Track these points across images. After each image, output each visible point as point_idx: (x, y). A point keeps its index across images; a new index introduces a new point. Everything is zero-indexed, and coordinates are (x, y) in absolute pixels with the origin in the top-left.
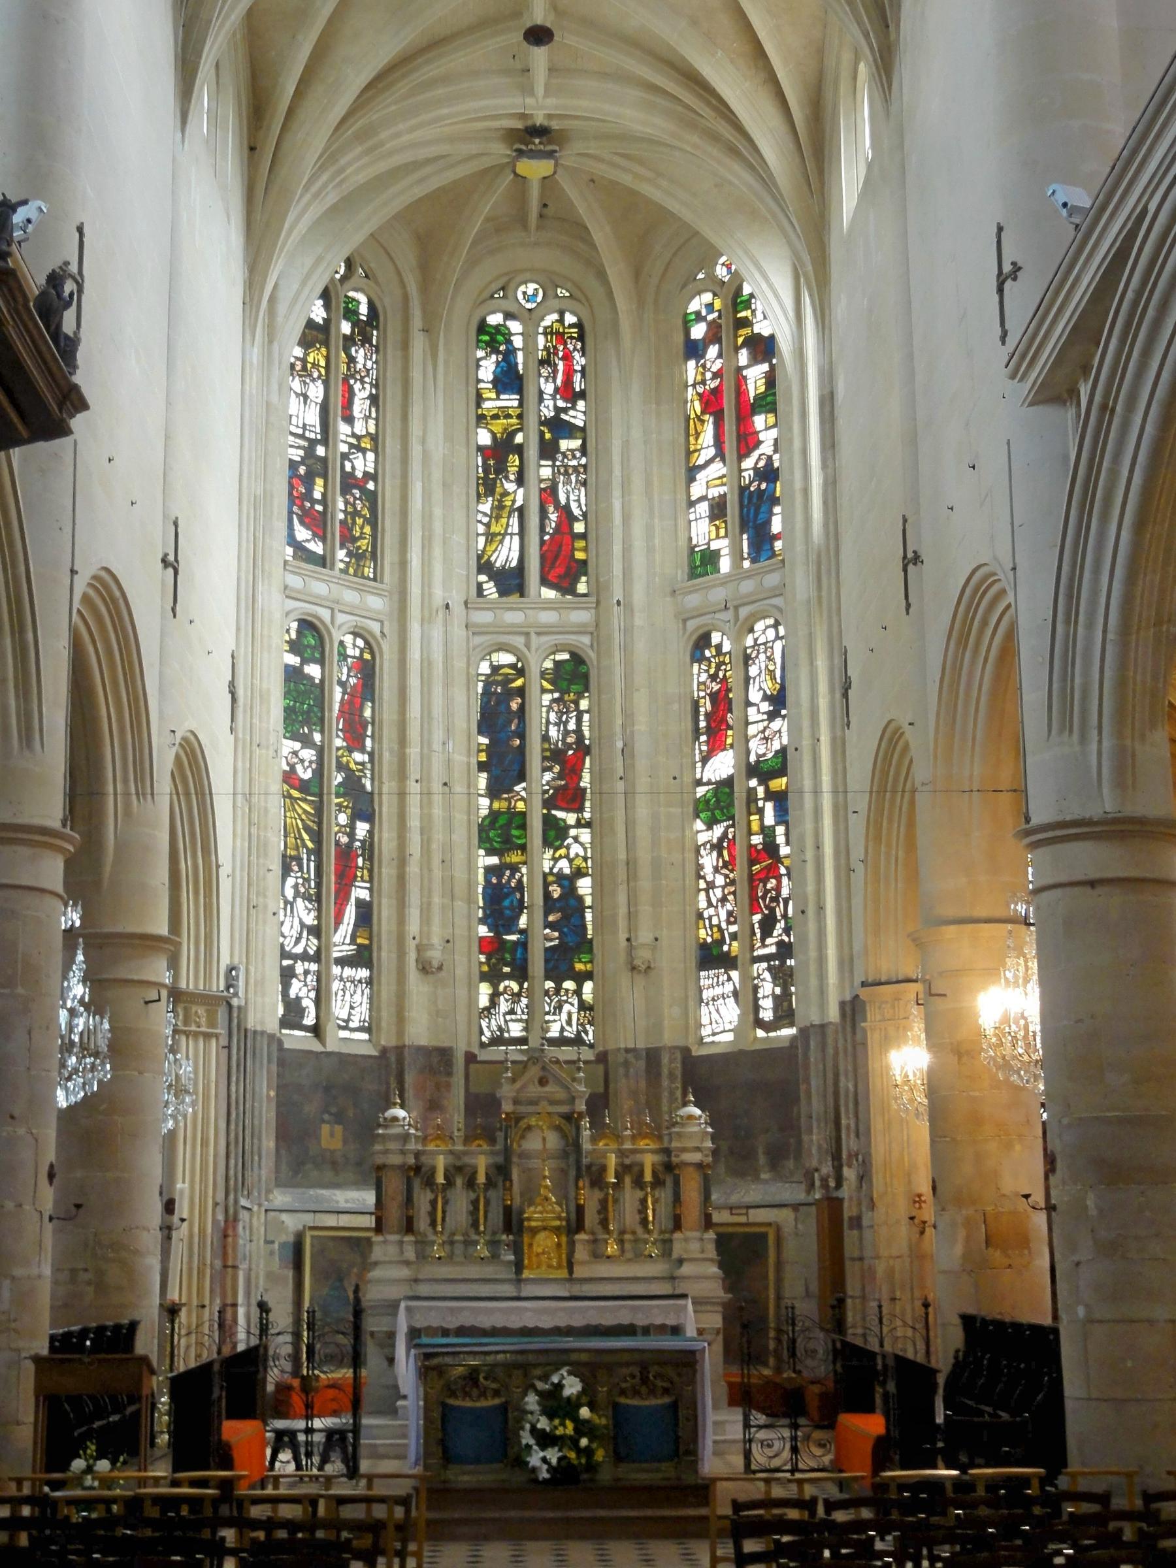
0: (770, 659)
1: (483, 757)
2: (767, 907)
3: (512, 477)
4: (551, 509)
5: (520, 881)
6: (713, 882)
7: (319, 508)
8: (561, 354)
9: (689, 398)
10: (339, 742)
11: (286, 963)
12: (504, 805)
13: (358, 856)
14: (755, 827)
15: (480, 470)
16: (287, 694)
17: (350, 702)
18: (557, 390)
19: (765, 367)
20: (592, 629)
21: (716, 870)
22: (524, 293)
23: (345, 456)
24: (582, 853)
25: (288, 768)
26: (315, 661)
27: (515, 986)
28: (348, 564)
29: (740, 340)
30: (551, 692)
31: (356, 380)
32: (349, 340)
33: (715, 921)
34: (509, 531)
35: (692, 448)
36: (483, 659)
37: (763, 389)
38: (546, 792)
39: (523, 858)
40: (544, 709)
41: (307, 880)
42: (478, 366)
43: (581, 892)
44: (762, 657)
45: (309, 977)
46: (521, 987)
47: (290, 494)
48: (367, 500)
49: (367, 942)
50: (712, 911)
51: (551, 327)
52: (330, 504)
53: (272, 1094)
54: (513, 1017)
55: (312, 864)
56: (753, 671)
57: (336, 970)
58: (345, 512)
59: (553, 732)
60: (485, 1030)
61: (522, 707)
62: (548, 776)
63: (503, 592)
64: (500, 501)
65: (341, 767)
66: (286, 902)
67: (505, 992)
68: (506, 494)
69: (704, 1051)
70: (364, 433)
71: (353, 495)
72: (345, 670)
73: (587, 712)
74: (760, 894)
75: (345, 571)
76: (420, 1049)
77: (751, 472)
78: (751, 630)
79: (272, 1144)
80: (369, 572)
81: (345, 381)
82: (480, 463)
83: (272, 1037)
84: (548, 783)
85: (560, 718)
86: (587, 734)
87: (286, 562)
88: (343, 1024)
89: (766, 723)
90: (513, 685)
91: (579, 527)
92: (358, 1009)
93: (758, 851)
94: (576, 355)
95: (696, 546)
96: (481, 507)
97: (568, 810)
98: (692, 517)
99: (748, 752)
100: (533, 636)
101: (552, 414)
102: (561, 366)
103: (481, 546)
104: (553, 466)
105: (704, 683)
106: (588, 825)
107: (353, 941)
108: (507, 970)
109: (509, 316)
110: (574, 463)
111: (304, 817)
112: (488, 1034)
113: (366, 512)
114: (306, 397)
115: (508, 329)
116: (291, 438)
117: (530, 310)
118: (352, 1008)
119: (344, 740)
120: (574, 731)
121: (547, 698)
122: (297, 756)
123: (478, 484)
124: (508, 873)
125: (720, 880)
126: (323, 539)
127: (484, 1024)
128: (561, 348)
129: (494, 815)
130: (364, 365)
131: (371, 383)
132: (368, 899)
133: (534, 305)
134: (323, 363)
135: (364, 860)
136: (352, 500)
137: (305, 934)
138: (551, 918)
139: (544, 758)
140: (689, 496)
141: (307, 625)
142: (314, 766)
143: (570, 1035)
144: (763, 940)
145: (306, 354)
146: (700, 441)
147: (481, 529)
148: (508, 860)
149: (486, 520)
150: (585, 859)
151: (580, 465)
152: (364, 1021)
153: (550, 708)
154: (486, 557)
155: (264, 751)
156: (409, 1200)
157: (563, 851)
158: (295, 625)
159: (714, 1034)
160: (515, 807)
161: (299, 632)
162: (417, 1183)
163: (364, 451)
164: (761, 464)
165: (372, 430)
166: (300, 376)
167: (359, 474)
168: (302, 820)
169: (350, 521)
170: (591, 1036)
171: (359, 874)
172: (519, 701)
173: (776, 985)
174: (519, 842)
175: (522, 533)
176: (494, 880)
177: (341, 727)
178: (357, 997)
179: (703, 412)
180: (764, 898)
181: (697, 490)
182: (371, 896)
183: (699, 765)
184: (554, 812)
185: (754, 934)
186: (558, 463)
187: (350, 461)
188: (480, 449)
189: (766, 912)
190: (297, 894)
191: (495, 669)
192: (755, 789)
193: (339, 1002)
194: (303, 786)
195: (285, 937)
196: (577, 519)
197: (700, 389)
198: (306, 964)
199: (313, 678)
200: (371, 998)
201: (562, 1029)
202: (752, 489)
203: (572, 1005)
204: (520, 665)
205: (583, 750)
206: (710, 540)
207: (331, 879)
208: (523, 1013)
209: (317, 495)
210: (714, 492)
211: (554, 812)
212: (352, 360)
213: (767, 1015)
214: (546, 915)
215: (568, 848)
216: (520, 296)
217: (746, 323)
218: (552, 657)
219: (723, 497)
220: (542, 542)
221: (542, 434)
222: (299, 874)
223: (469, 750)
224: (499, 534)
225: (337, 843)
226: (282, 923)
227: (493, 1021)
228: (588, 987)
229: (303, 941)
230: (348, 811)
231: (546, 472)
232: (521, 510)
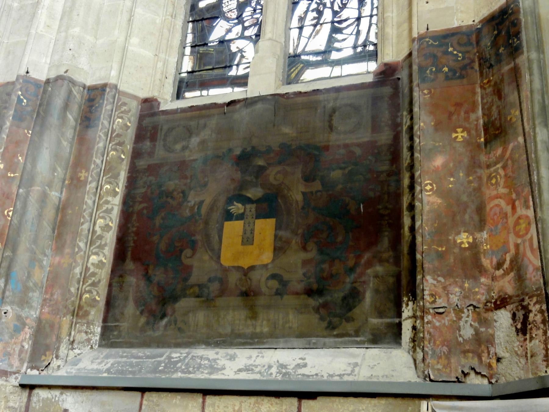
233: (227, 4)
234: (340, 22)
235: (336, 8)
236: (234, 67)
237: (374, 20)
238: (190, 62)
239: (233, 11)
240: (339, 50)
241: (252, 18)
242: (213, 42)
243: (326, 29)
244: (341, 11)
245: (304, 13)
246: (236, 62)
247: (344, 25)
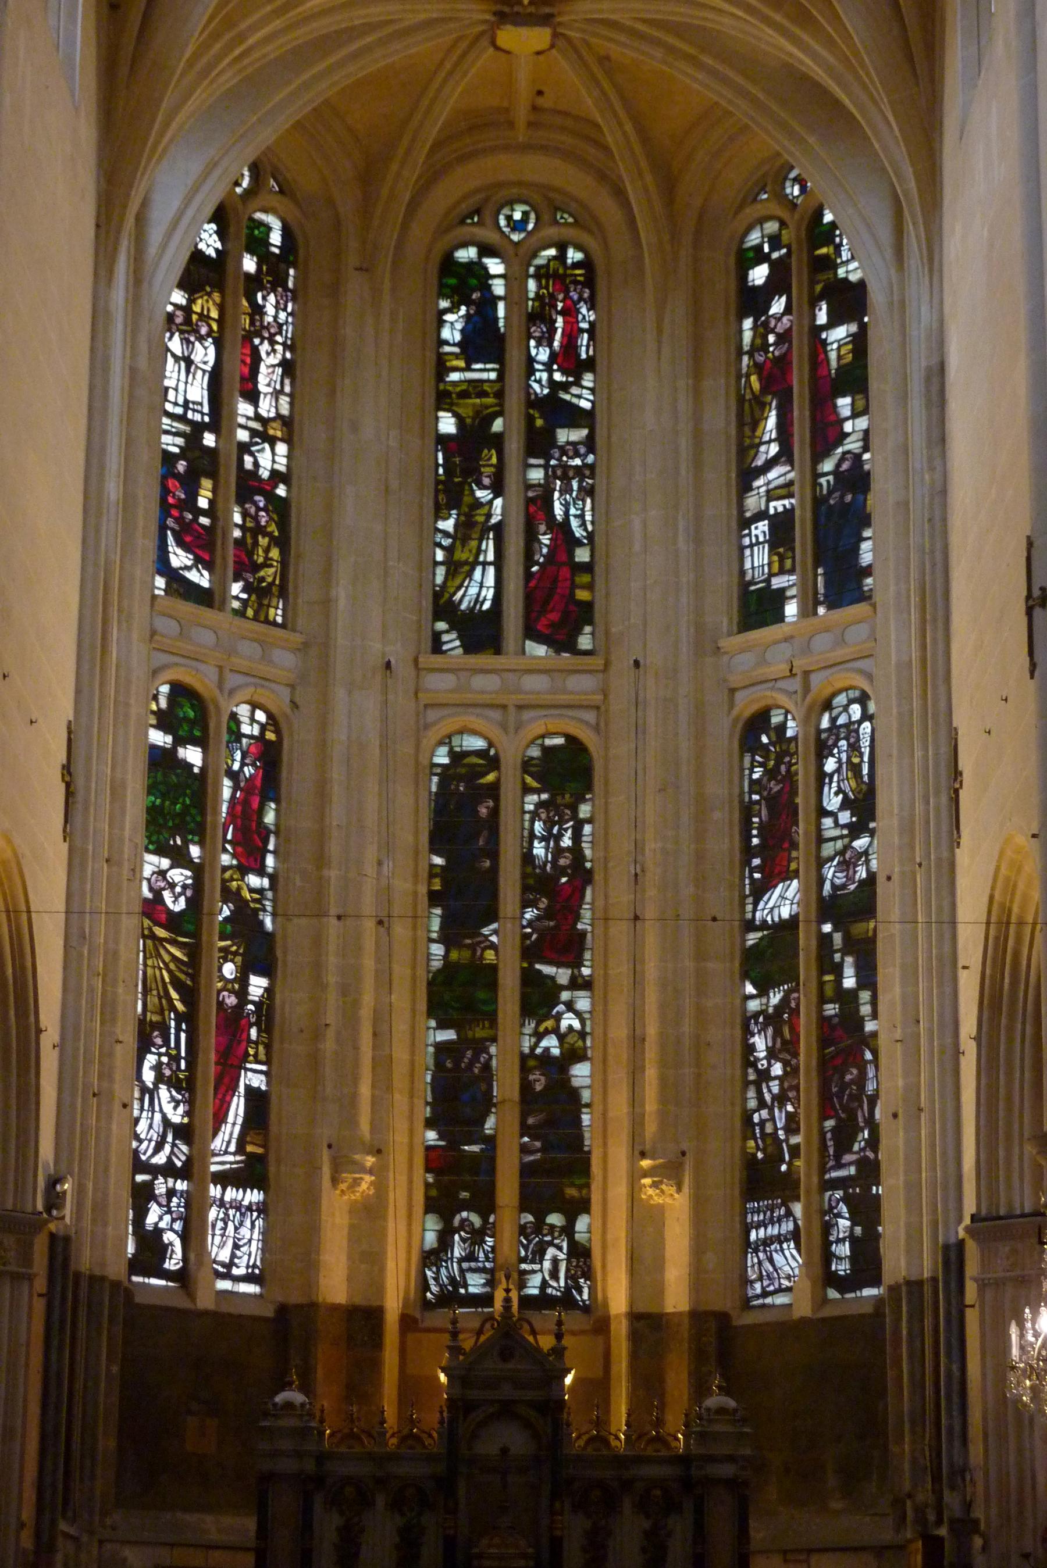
0: (854, 747)
1: (437, 886)
2: (844, 1109)
3: (486, 481)
4: (542, 528)
5: (487, 1067)
6: (768, 1071)
7: (204, 521)
8: (560, 305)
9: (744, 370)
10: (226, 859)
11: (140, 1178)
12: (466, 954)
13: (251, 1025)
14: (829, 991)
15: (441, 471)
16: (151, 789)
17: (246, 802)
18: (553, 357)
19: (854, 328)
20: (598, 698)
21: (772, 1054)
22: (509, 218)
23: (244, 448)
24: (576, 1024)
25: (150, 895)
26: (195, 742)
27: (476, 1220)
28: (245, 603)
29: (818, 288)
30: (538, 792)
31: (263, 339)
32: (253, 283)
33: (769, 1128)
34: (481, 559)
35: (747, 441)
36: (441, 743)
37: (850, 357)
38: (527, 936)
39: (491, 1032)
40: (527, 817)
41: (176, 1059)
42: (441, 323)
43: (576, 1082)
44: (843, 743)
46: (485, 1221)
47: (163, 500)
48: (275, 511)
49: (260, 1151)
50: (764, 1113)
51: (547, 266)
52: (220, 514)
53: (115, 1369)
54: (473, 1265)
55: (183, 1035)
56: (830, 765)
57: (215, 1191)
58: (242, 527)
59: (539, 850)
60: (432, 1282)
61: (495, 812)
62: (530, 914)
63: (470, 647)
64: (469, 516)
65: (229, 895)
66: (144, 1089)
67: (462, 1227)
68: (477, 504)
69: (749, 1319)
70: (272, 415)
71: (255, 504)
72: (238, 755)
73: (589, 821)
74: (834, 1090)
75: (241, 613)
76: (335, 1308)
77: (831, 478)
78: (828, 706)
79: (112, 1444)
80: (277, 615)
81: (248, 338)
82: (441, 461)
83: (116, 1285)
84: (530, 924)
85: (549, 830)
86: (588, 853)
87: (154, 597)
88: (221, 1269)
89: (846, 840)
90: (482, 781)
91: (582, 555)
92: (244, 1249)
93: (833, 1028)
94: (584, 310)
95: (753, 582)
96: (441, 525)
97: (559, 965)
98: (746, 541)
99: (821, 881)
100: (512, 710)
101: (546, 391)
102: (560, 322)
103: (439, 579)
104: (546, 467)
105: (758, 781)
106: (586, 985)
107: (240, 1149)
108: (465, 1195)
109: (486, 250)
110: (578, 462)
111: (172, 966)
112: (434, 1289)
113: (273, 528)
114: (189, 362)
115: (486, 269)
116: (165, 420)
117: (517, 244)
118: (236, 1246)
119: (234, 856)
120: (568, 849)
121: (531, 801)
122: (165, 878)
123: (437, 491)
124: (469, 1054)
125: (777, 1069)
126: (209, 566)
127: (429, 1273)
128: (561, 296)
129: (449, 967)
130: (276, 317)
131: (284, 344)
132: (263, 1088)
133: (522, 235)
134: (214, 314)
135: (259, 1031)
136: (253, 510)
137: (170, 1138)
138: (531, 1121)
139: (525, 888)
140: (741, 508)
141: (180, 691)
142: (189, 893)
143: (554, 1292)
144: (838, 1157)
145: (191, 301)
146: (758, 433)
147: (440, 555)
148: (470, 1034)
149: (447, 542)
150: (582, 1034)
151: (585, 465)
152: (254, 1266)
153: (535, 815)
154: (447, 596)
155: (115, 869)
156: (307, 1526)
157: (549, 1024)
158: (165, 689)
159: (765, 1294)
160: (482, 957)
161: (171, 697)
162: (318, 1501)
163: (272, 441)
164: (845, 466)
165: (285, 410)
166: (181, 332)
167: (265, 474)
168: (169, 971)
169: (249, 541)
170: (585, 1296)
171: (251, 1052)
172: (491, 803)
173: (854, 1223)
174: (486, 1008)
175: (499, 563)
176: (449, 1065)
177: (229, 837)
178: (245, 1232)
179: (764, 390)
180: (840, 1095)
181: (753, 503)
182: (268, 1084)
183: (750, 900)
184: (538, 966)
185: (824, 1146)
186: (553, 462)
187: (252, 454)
188: (443, 440)
189: (843, 1116)
190: (159, 1079)
191: (457, 757)
192: (829, 936)
193: (217, 1239)
194: (173, 922)
195: (141, 1141)
196: (578, 543)
197: (760, 358)
198: (171, 1181)
199: (192, 766)
200: (264, 1233)
201: (544, 1284)
202: (832, 502)
203: (560, 1249)
204: (492, 752)
205: (582, 876)
206: (771, 575)
207: (209, 1057)
208: (487, 1259)
209: (203, 503)
210: (777, 506)
211: (538, 966)
212: (258, 310)
213: (842, 1268)
214: (524, 1116)
215: (558, 1018)
216: (502, 222)
217: (829, 264)
218: (539, 741)
219: (789, 512)
220: (528, 576)
221: (530, 420)
222: (163, 1050)
223: (416, 875)
224: (466, 563)
225: (221, 1004)
226: (137, 1121)
227: (443, 1271)
228: (582, 1224)
229: (167, 1148)
230: (239, 959)
231: (536, 475)
232: (498, 528)
234: (239, 1240)
235: (237, 1223)
240: (238, 1267)
243: (230, 1243)
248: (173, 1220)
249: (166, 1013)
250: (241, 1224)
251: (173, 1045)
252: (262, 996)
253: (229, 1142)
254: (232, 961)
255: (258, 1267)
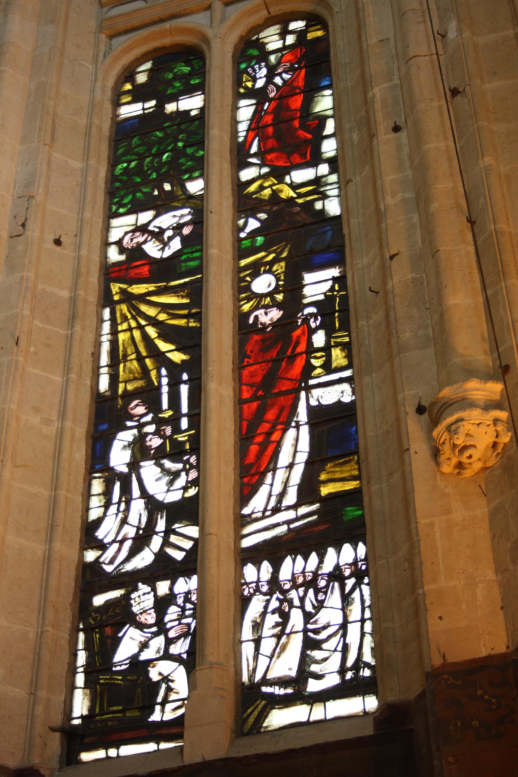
45: (173, 612)
152: (359, 664)
195: (102, 547)
229: (156, 542)
233: (137, 599)
234: (316, 632)
235: (309, 608)
236: (158, 708)
237: (368, 626)
238: (86, 700)
239: (148, 612)
240: (319, 677)
241: (180, 624)
242: (121, 665)
244: (316, 613)
245: (260, 615)
246: (159, 699)
247: (323, 635)
248: (169, 642)
249: (153, 374)
250: (320, 605)
251: (165, 405)
252: (332, 289)
253: (282, 495)
254: (269, 272)
255: (368, 665)
